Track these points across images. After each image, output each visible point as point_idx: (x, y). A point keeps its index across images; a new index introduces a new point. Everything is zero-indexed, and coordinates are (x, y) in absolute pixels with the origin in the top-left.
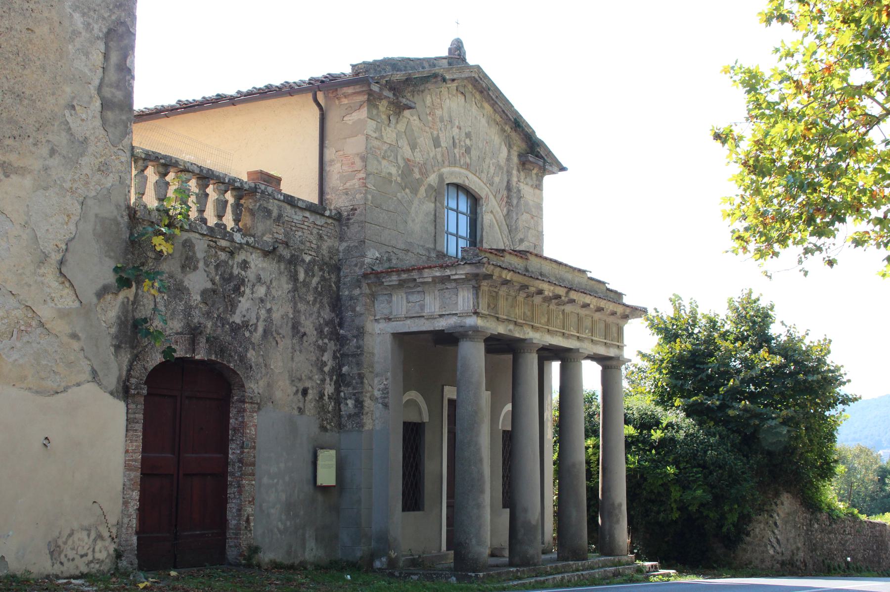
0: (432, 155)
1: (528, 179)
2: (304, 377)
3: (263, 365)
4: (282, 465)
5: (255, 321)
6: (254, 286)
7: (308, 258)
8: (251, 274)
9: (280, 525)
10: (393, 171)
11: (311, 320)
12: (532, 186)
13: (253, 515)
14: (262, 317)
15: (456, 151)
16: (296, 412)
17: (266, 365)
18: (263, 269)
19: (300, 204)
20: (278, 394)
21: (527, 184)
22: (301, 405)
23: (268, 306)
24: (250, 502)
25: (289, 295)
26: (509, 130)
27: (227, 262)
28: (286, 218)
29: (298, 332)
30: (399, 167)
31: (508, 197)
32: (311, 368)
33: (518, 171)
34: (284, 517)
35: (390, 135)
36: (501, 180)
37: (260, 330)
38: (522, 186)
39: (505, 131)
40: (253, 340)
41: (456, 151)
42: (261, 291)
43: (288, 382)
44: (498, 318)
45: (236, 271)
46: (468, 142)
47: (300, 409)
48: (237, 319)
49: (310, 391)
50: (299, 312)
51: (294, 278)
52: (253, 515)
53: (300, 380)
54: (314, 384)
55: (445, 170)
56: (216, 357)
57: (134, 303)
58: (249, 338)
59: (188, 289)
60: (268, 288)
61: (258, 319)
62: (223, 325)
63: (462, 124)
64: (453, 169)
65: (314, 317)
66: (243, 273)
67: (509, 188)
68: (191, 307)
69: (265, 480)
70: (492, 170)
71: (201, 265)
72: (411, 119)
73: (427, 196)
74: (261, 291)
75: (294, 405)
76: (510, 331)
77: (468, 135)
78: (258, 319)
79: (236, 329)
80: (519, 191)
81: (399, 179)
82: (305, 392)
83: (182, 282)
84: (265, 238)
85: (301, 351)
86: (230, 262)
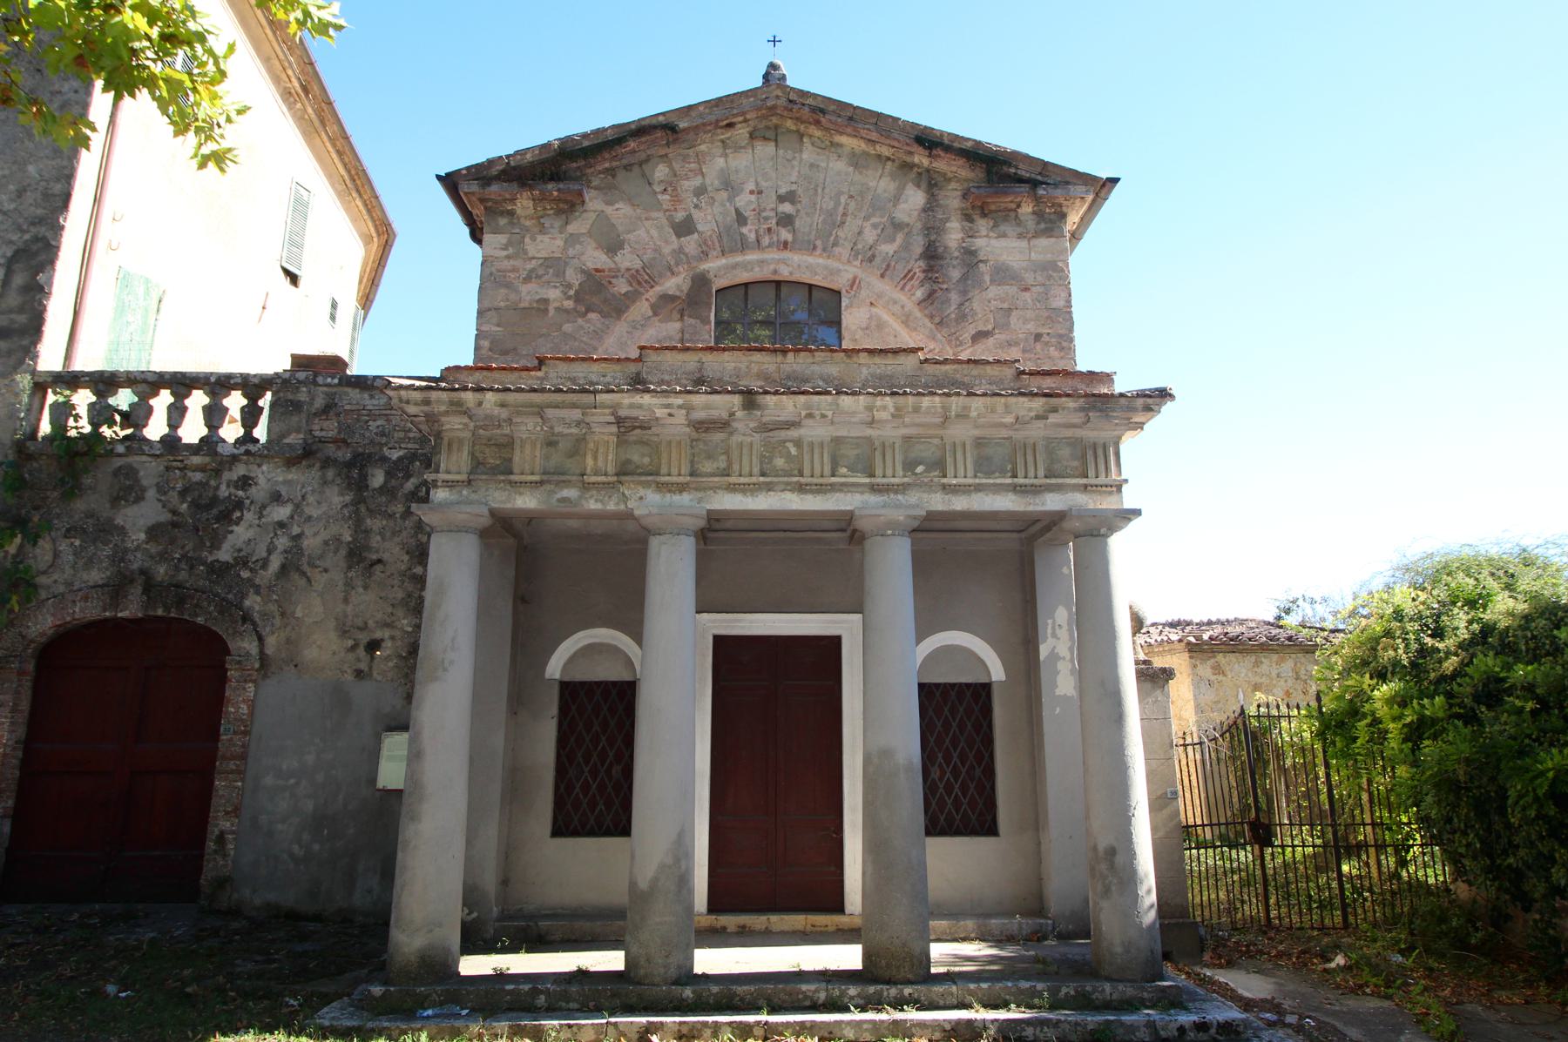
0: (667, 250)
1: (1002, 228)
2: (371, 623)
3: (277, 614)
4: (310, 759)
5: (264, 554)
6: (264, 507)
7: (395, 455)
8: (258, 492)
9: (296, 848)
10: (554, 294)
11: (397, 539)
12: (1020, 236)
13: (233, 832)
14: (280, 548)
15: (745, 230)
16: (349, 677)
17: (283, 614)
18: (285, 482)
19: (378, 383)
20: (310, 654)
21: (1004, 235)
22: (363, 666)
23: (296, 530)
24: (227, 813)
25: (346, 511)
26: (926, 162)
27: (207, 483)
28: (348, 407)
29: (361, 560)
30: (569, 286)
31: (929, 269)
32: (390, 610)
33: (968, 218)
34: (306, 837)
35: (545, 245)
36: (906, 247)
37: (275, 563)
38: (979, 243)
39: (911, 166)
40: (257, 581)
41: (745, 230)
42: (282, 513)
43: (333, 635)
44: (513, 484)
45: (224, 492)
46: (787, 208)
47: (359, 674)
48: (224, 555)
49: (389, 644)
50: (367, 532)
51: (359, 486)
52: (233, 832)
53: (364, 628)
54: (398, 633)
55: (712, 265)
56: (167, 608)
57: (15, 556)
58: (249, 580)
59: (123, 528)
60: (297, 506)
61: (270, 552)
62: (192, 567)
63: (764, 184)
64: (739, 258)
65: (404, 533)
66: (240, 493)
67: (932, 255)
68: (126, 550)
69: (269, 781)
70: (870, 236)
71: (151, 493)
72: (609, 210)
73: (655, 314)
74: (282, 513)
75: (345, 667)
76: (564, 500)
77: (790, 197)
78: (270, 552)
79: (220, 571)
80: (970, 253)
81: (569, 304)
82: (373, 646)
83: (110, 520)
84: (286, 441)
85: (366, 588)
86: (213, 483)
